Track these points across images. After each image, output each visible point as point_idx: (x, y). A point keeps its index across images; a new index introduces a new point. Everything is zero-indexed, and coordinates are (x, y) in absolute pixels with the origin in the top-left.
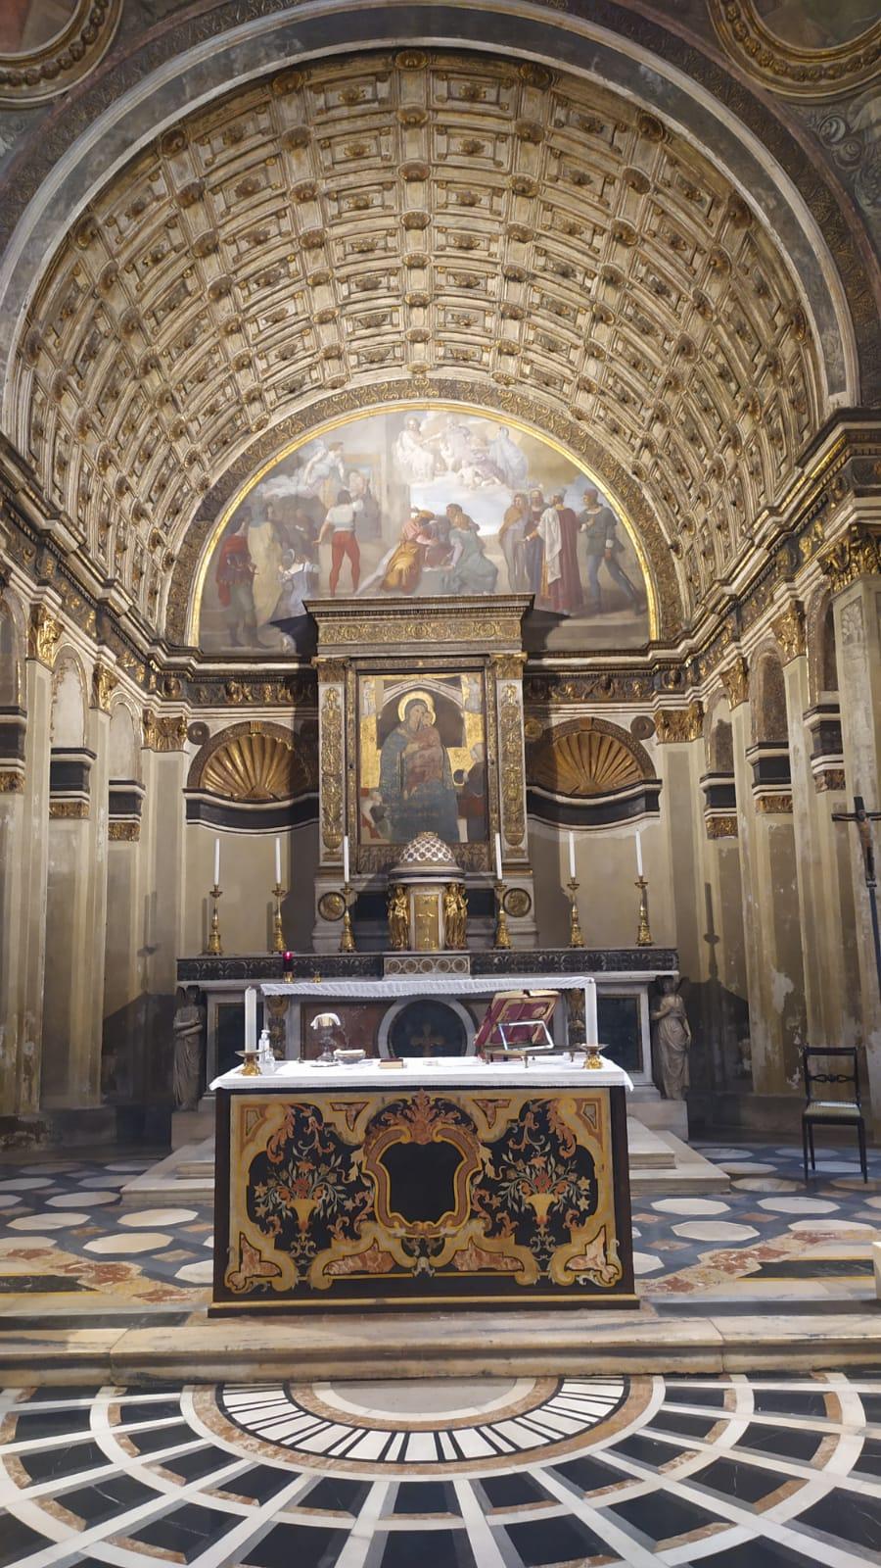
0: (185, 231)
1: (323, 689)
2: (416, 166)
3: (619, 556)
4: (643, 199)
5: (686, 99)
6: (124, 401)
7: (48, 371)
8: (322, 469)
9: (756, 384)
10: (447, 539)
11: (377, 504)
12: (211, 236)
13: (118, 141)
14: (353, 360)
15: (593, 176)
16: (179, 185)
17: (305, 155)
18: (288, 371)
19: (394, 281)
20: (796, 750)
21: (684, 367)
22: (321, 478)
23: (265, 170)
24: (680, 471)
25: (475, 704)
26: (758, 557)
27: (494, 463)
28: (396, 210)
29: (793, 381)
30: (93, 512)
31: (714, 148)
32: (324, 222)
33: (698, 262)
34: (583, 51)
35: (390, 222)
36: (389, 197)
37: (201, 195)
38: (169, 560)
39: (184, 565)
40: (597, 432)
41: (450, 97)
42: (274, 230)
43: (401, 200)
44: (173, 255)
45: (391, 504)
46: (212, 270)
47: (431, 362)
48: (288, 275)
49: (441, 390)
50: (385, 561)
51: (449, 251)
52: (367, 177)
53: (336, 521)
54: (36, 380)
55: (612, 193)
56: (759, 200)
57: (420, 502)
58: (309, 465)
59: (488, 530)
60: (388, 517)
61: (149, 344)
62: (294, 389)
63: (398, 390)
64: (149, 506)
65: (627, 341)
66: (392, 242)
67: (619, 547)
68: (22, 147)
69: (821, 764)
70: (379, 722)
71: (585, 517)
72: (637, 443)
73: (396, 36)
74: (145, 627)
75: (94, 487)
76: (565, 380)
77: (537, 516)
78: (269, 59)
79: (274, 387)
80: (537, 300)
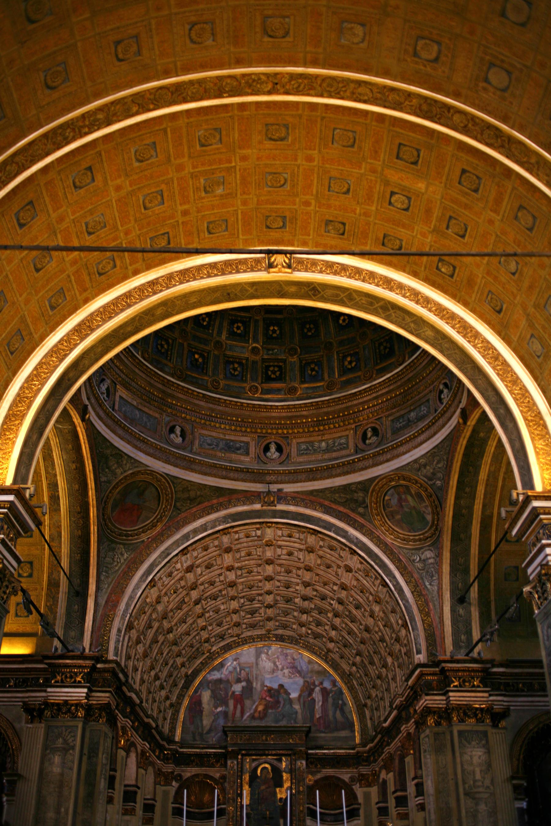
0: (186, 581)
1: (229, 762)
2: (270, 559)
3: (345, 708)
4: (351, 574)
5: (364, 544)
6: (159, 644)
7: (134, 634)
8: (231, 669)
9: (392, 645)
10: (278, 698)
11: (252, 683)
12: (194, 583)
13: (166, 554)
14: (244, 626)
15: (333, 565)
16: (185, 565)
17: (230, 555)
18: (219, 630)
19: (260, 598)
20: (410, 794)
21: (366, 635)
22: (230, 672)
23: (215, 560)
24: (366, 675)
25: (287, 770)
26: (395, 713)
27: (297, 668)
28: (262, 574)
29: (406, 645)
30: (144, 689)
31: (375, 562)
32: (236, 577)
33: (371, 598)
34: (329, 526)
35: (260, 577)
36: (260, 569)
37: (192, 568)
38: (172, 705)
39: (176, 707)
40: (336, 657)
41: (283, 536)
42: (217, 580)
43: (264, 571)
44: (181, 590)
45: (257, 683)
46: (195, 594)
47: (273, 627)
48: (222, 596)
49: (276, 638)
50: (254, 707)
51: (281, 588)
52: (252, 562)
53: (236, 690)
54: (130, 637)
55: (340, 571)
56: (390, 581)
57: (267, 683)
58: (226, 667)
59: (294, 695)
60: (255, 688)
61: (170, 622)
62: (222, 637)
63: (261, 638)
64: (165, 683)
65: (346, 624)
66: (260, 584)
67: (344, 704)
68: (132, 556)
69: (419, 800)
70: (250, 776)
71: (331, 691)
72: (351, 662)
73: (264, 518)
74: (160, 733)
75: (146, 677)
76: (323, 636)
77: (313, 690)
78: (220, 525)
79: (214, 636)
80: (313, 606)
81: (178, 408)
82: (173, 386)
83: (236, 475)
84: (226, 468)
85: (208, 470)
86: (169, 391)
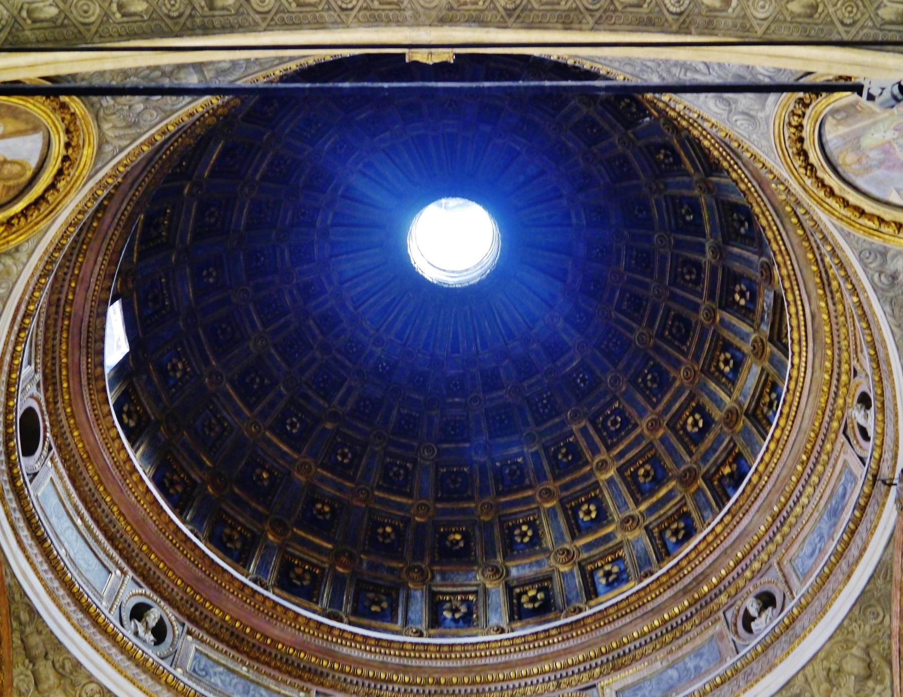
81: (730, 578)
82: (682, 569)
83: (858, 540)
84: (839, 555)
85: (822, 597)
86: (687, 580)
